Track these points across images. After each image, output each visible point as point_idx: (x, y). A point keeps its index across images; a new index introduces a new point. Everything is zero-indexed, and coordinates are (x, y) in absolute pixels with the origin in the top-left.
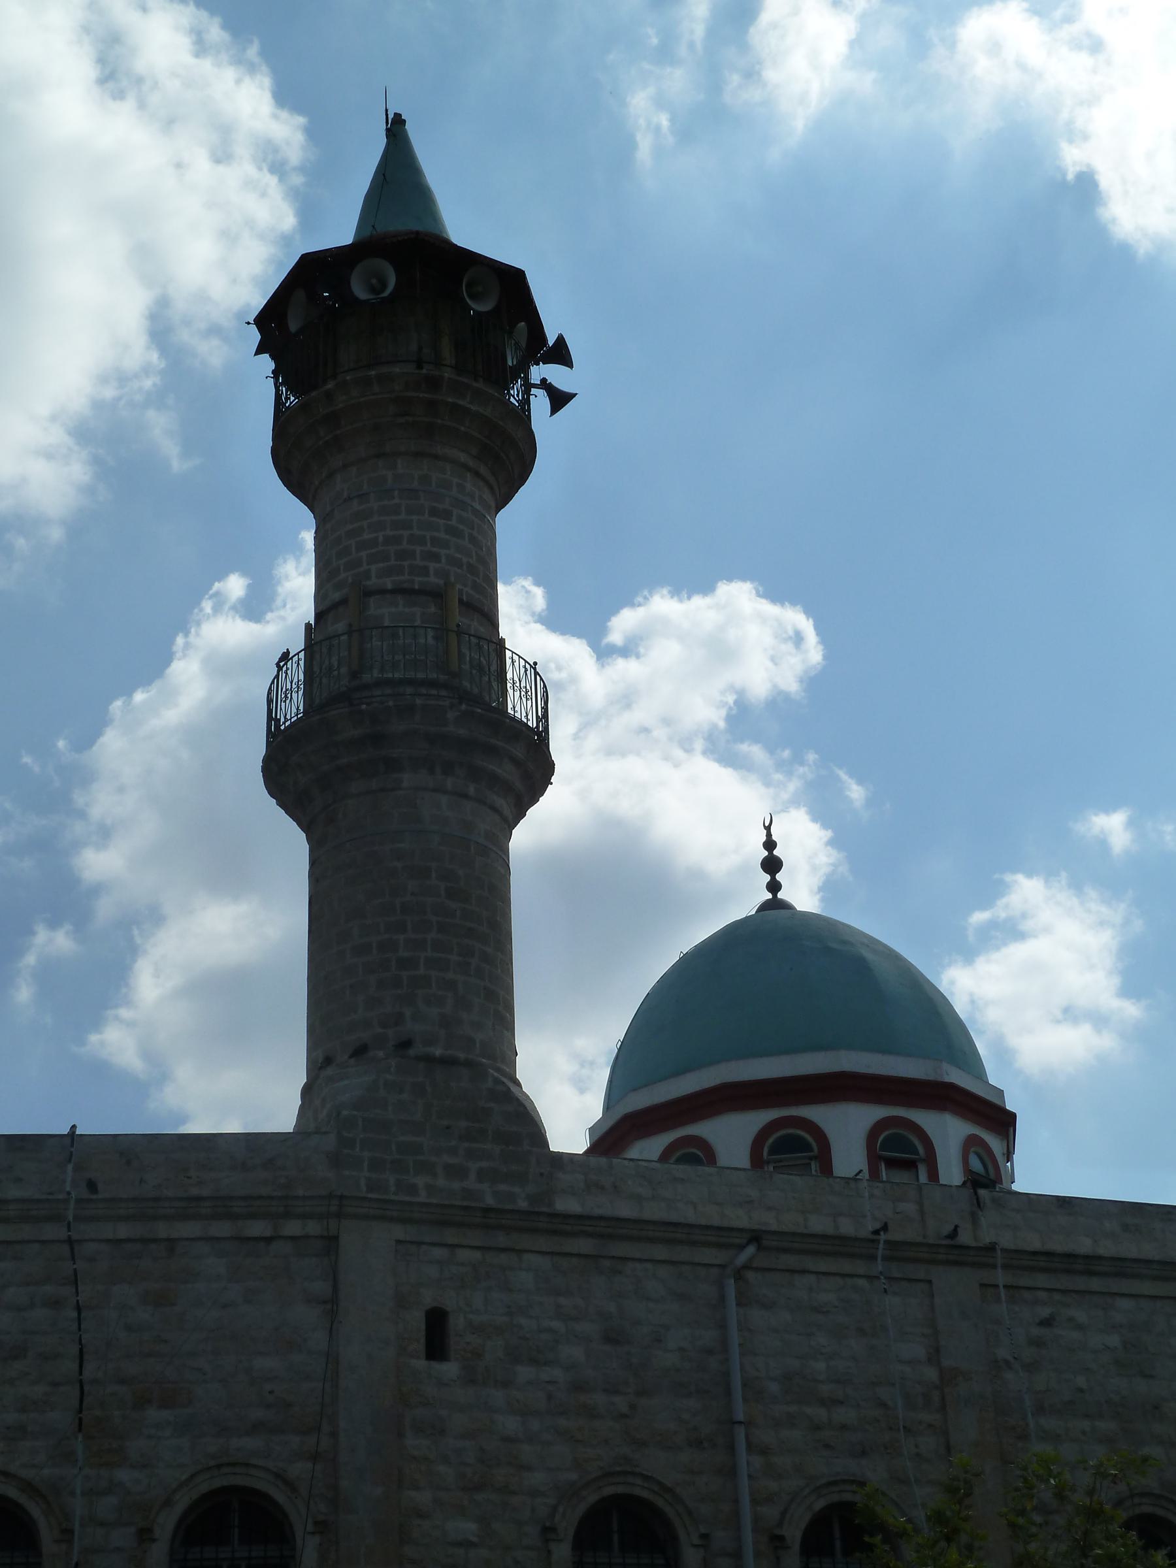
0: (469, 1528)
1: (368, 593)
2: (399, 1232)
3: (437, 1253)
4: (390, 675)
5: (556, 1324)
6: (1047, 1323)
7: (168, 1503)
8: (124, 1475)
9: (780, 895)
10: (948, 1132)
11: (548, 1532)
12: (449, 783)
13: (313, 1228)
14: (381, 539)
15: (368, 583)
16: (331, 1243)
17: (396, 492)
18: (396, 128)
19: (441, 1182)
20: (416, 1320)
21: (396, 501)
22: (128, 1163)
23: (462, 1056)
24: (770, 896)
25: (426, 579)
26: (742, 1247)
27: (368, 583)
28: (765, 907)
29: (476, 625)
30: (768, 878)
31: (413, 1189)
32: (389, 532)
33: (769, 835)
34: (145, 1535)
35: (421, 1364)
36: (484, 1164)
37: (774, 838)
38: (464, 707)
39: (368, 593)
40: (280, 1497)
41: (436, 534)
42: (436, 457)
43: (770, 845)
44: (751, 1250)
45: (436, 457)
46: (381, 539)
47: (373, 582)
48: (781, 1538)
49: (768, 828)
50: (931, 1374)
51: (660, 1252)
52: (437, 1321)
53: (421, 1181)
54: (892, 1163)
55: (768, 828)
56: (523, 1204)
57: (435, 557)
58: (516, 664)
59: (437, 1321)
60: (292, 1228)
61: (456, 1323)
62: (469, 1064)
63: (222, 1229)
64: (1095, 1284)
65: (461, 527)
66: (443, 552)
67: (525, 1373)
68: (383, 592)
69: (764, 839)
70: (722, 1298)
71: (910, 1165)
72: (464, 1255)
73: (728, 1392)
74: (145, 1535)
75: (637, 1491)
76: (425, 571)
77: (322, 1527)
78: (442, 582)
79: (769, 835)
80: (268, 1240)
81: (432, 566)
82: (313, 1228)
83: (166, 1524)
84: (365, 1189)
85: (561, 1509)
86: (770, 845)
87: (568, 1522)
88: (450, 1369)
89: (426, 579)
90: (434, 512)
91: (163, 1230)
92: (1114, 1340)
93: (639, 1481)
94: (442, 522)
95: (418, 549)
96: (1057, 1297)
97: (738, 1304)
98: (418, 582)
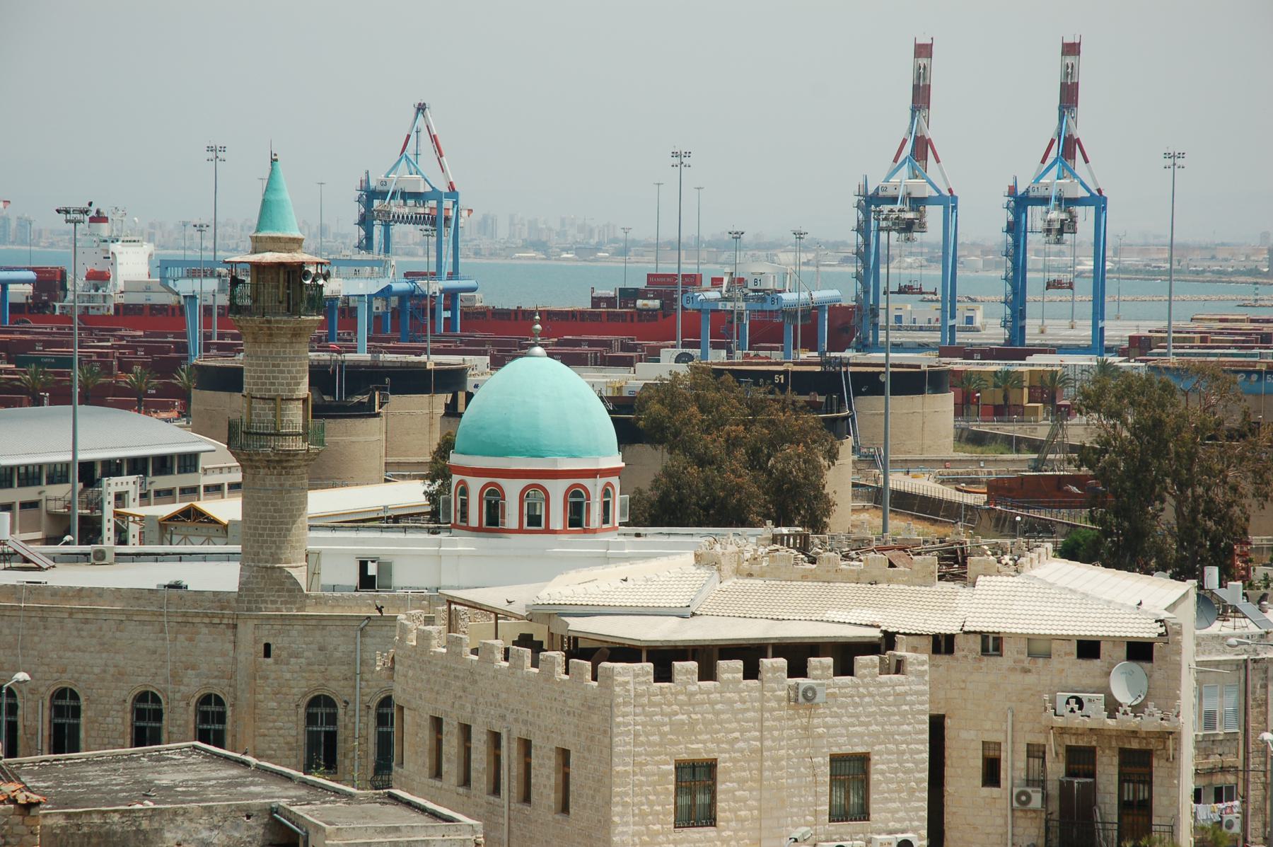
2: (256, 622)
8: (182, 688)
11: (298, 706)
16: (235, 626)
20: (262, 648)
34: (188, 704)
35: (262, 659)
52: (267, 648)
57: (273, 384)
59: (267, 648)
61: (273, 647)
67: (293, 660)
74: (188, 704)
77: (232, 705)
83: (193, 701)
88: (270, 660)
90: (274, 365)
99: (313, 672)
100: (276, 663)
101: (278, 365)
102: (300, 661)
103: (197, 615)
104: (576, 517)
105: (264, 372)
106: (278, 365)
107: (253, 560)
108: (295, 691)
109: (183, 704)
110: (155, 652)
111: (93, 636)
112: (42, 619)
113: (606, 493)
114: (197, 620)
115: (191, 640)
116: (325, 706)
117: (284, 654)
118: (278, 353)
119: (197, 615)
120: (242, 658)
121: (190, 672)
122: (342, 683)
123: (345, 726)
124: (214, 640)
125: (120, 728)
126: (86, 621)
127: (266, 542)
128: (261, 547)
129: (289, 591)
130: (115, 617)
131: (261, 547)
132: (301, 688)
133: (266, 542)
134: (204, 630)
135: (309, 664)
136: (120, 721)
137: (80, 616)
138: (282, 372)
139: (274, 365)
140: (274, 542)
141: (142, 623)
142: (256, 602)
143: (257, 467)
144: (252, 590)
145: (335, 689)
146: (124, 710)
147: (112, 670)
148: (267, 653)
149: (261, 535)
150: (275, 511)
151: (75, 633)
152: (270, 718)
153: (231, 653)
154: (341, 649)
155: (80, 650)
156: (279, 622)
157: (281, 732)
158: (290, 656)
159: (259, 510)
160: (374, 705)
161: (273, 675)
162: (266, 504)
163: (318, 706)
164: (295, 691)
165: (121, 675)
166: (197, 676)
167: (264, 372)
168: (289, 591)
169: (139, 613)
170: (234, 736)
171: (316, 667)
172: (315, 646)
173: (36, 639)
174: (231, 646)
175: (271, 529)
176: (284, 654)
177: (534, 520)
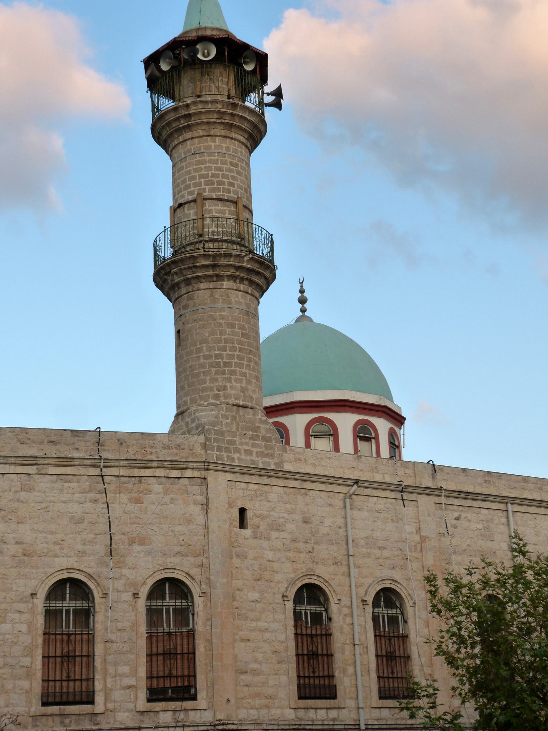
0: (255, 596)
1: (206, 199)
2: (229, 476)
3: (243, 485)
4: (216, 237)
5: (286, 515)
6: (457, 519)
7: (144, 583)
8: (125, 571)
9: (306, 314)
10: (382, 425)
12: (242, 287)
14: (210, 175)
15: (205, 194)
17: (216, 154)
19: (243, 457)
21: (216, 158)
22: (121, 444)
23: (250, 405)
24: (301, 314)
25: (229, 195)
26: (352, 486)
27: (205, 194)
28: (298, 320)
29: (246, 215)
30: (300, 306)
31: (233, 459)
32: (213, 172)
33: (302, 286)
34: (135, 595)
35: (238, 530)
36: (259, 450)
37: (304, 288)
38: (251, 256)
39: (206, 199)
41: (233, 174)
42: (232, 138)
43: (302, 291)
44: (355, 487)
45: (232, 138)
46: (210, 175)
47: (206, 194)
48: (366, 601)
49: (301, 283)
50: (417, 538)
51: (322, 487)
53: (236, 456)
55: (301, 283)
56: (273, 467)
57: (232, 184)
58: (257, 230)
60: (189, 473)
61: (249, 514)
62: (252, 408)
63: (160, 473)
64: (475, 504)
65: (242, 171)
66: (236, 182)
67: (274, 534)
68: (212, 199)
69: (299, 288)
70: (345, 506)
71: (368, 439)
72: (251, 486)
73: (347, 544)
75: (316, 582)
76: (229, 191)
78: (236, 197)
79: (302, 286)
80: (179, 478)
81: (232, 189)
82: (196, 474)
83: (144, 591)
84: (215, 459)
85: (289, 589)
86: (302, 291)
87: (291, 595)
88: (247, 532)
89: (229, 195)
91: (136, 472)
92: (480, 526)
93: (316, 578)
94: (235, 168)
95: (226, 180)
96: (461, 508)
97: (351, 509)
98: (226, 196)
99: (299, 551)
101: (236, 165)
102: (283, 535)
103: (148, 464)
105: (220, 169)
107: (217, 397)
108: (278, 577)
109: (127, 597)
110: (81, 521)
115: (138, 501)
117: (263, 526)
120: (213, 525)
121: (136, 548)
122: (332, 568)
123: (342, 628)
124: (172, 501)
125: (26, 639)
127: (233, 373)
128: (229, 380)
130: (19, 469)
131: (229, 380)
132: (287, 577)
133: (233, 373)
134: (157, 487)
135: (294, 541)
136: (24, 628)
138: (238, 173)
139: (232, 164)
140: (244, 374)
142: (228, 450)
143: (219, 277)
144: (222, 433)
145: (326, 575)
146: (32, 612)
148: (243, 524)
149: (226, 364)
150: (243, 335)
152: (252, 615)
153: (201, 520)
154: (328, 522)
156: (257, 479)
157: (267, 635)
159: (221, 334)
161: (251, 554)
162: (232, 326)
164: (278, 577)
167: (220, 169)
170: (210, 641)
172: (298, 517)
174: (197, 510)
175: (240, 358)
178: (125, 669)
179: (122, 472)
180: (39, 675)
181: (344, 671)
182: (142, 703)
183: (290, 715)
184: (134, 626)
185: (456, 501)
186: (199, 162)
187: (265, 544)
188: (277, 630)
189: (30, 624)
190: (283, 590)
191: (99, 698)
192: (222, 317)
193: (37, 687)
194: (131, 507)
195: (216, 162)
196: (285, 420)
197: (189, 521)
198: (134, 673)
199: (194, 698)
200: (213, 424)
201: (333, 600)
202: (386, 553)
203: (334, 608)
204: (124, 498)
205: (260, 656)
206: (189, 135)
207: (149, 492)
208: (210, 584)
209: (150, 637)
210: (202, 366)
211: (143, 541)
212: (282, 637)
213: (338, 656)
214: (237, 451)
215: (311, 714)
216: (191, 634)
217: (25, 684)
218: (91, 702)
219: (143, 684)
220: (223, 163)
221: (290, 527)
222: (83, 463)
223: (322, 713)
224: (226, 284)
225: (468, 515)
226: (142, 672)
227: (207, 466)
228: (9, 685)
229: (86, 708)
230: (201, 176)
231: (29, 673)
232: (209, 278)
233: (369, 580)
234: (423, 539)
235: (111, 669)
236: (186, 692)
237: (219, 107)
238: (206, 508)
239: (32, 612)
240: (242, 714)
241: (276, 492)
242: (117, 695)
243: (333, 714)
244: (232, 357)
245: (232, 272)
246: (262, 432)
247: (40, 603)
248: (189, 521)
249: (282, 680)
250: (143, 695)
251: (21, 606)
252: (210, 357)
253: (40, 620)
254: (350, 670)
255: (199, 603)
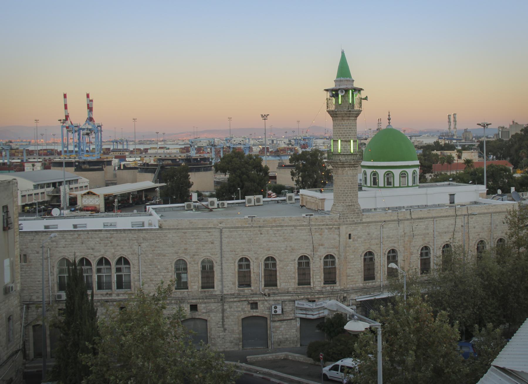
0: (353, 256)
2: (346, 226)
8: (318, 253)
11: (361, 256)
13: (337, 227)
16: (339, 228)
18: (343, 53)
20: (348, 235)
31: (347, 221)
34: (320, 259)
35: (348, 240)
40: (334, 255)
43: (389, 116)
50: (403, 233)
52: (350, 235)
54: (402, 177)
57: (349, 135)
59: (350, 235)
60: (335, 227)
61: (352, 235)
63: (327, 227)
67: (359, 239)
74: (320, 259)
82: (337, 227)
86: (389, 116)
88: (351, 240)
91: (321, 227)
99: (366, 243)
100: (353, 241)
101: (351, 128)
103: (323, 225)
104: (389, 184)
105: (346, 131)
106: (351, 128)
107: (343, 203)
108: (360, 251)
109: (318, 259)
110: (306, 240)
111: (281, 236)
112: (259, 231)
113: (414, 173)
114: (324, 227)
115: (321, 235)
116: (330, 258)
117: (356, 237)
118: (351, 123)
119: (323, 225)
121: (321, 247)
126: (278, 230)
129: (357, 213)
132: (362, 250)
134: (326, 231)
135: (365, 240)
136: (293, 268)
137: (275, 228)
138: (352, 131)
140: (351, 195)
141: (301, 229)
142: (346, 218)
143: (345, 167)
144: (344, 214)
145: (374, 248)
146: (295, 264)
147: (289, 248)
148: (350, 238)
149: (346, 193)
151: (274, 235)
153: (338, 239)
155: (275, 241)
158: (358, 238)
159: (345, 184)
160: (387, 253)
162: (348, 181)
163: (302, 259)
164: (360, 251)
165: (293, 250)
166: (324, 248)
167: (346, 131)
168: (357, 213)
169: (300, 226)
171: (367, 241)
172: (366, 234)
173: (257, 239)
174: (337, 236)
176: (356, 237)
177: (389, 183)
178: (318, 277)
179: (317, 227)
180: (297, 279)
181: (377, 273)
182: (322, 285)
183: (361, 285)
184: (320, 267)
185: (417, 221)
186: (340, 128)
187: (356, 242)
188: (359, 264)
189: (294, 267)
190: (361, 253)
191: (312, 284)
192: (345, 179)
193: (297, 281)
194: (319, 236)
195: (344, 128)
196: (378, 171)
197: (335, 239)
198: (320, 278)
199: (336, 283)
200: (342, 212)
201: (375, 255)
202: (393, 239)
203: (376, 257)
204: (317, 234)
205: (353, 272)
206: (337, 119)
207: (324, 232)
208: (340, 255)
209: (324, 269)
210: (339, 193)
211: (322, 245)
212: (360, 266)
213: (376, 269)
214: (349, 218)
215: (367, 284)
216: (335, 268)
217: (294, 281)
218: (310, 284)
219: (323, 280)
220: (347, 128)
221: (364, 237)
222: (306, 226)
223: (370, 284)
224: (347, 169)
225: (421, 224)
226: (322, 278)
227: (340, 225)
228: (290, 281)
229: (309, 286)
230: (340, 133)
231: (295, 278)
232: (342, 167)
233: (386, 248)
234: (405, 234)
235: (315, 277)
236: (334, 282)
237: (345, 112)
238: (339, 235)
239: (295, 264)
240: (348, 286)
241: (360, 227)
242: (316, 283)
243: (374, 284)
244: (348, 191)
245: (348, 166)
246: (357, 211)
247: (296, 262)
248: (335, 239)
249: (360, 277)
250: (322, 283)
251: (292, 262)
252: (341, 191)
253: (297, 266)
254: (379, 272)
255: (337, 261)
